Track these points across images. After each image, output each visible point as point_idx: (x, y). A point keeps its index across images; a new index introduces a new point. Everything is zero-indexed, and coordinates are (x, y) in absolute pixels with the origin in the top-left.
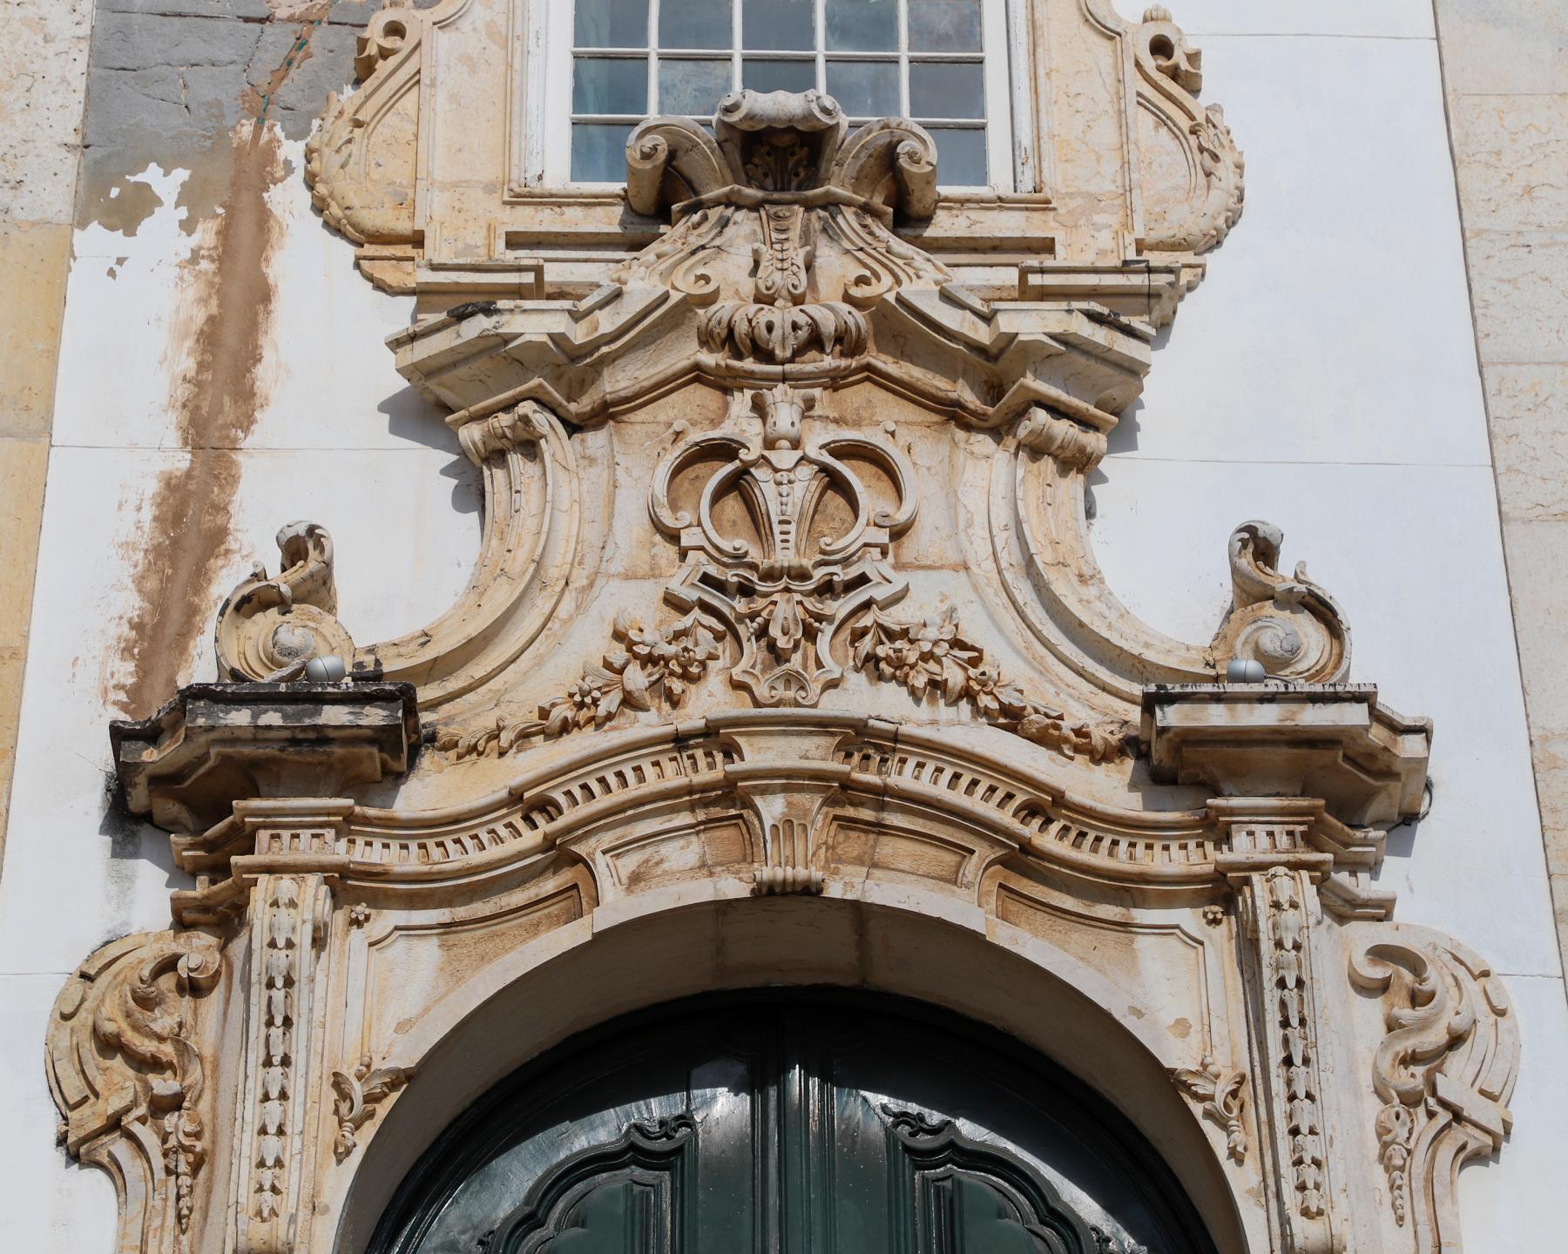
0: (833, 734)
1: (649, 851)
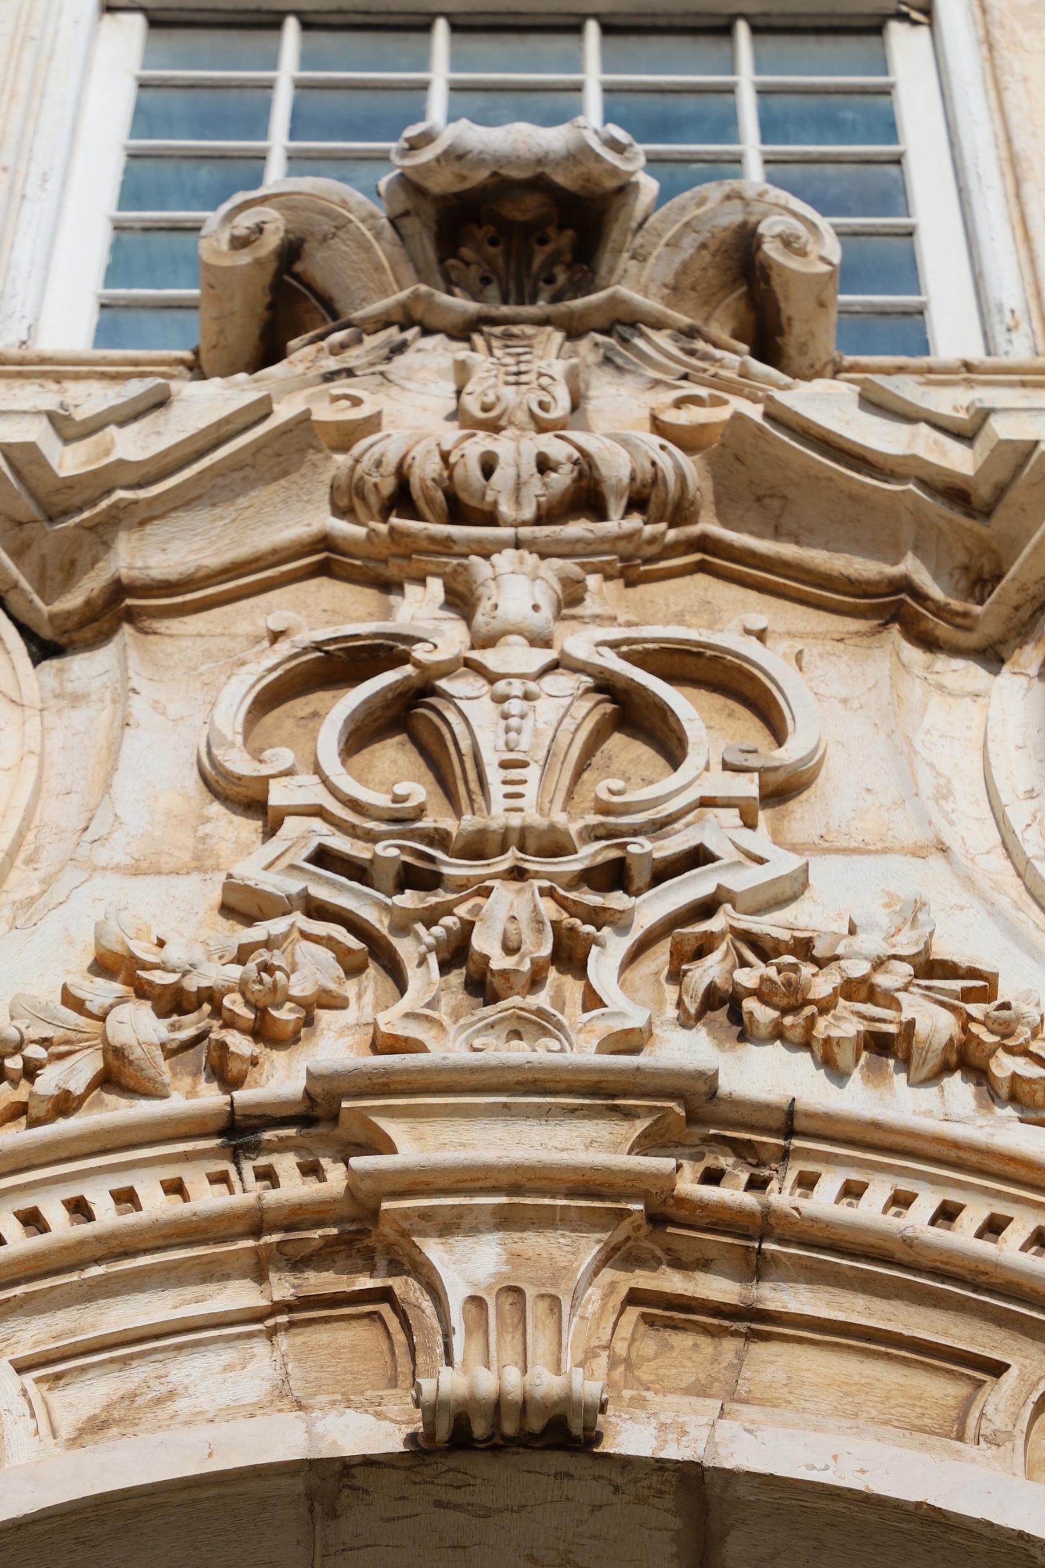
0: (628, 1114)
1: (138, 1374)
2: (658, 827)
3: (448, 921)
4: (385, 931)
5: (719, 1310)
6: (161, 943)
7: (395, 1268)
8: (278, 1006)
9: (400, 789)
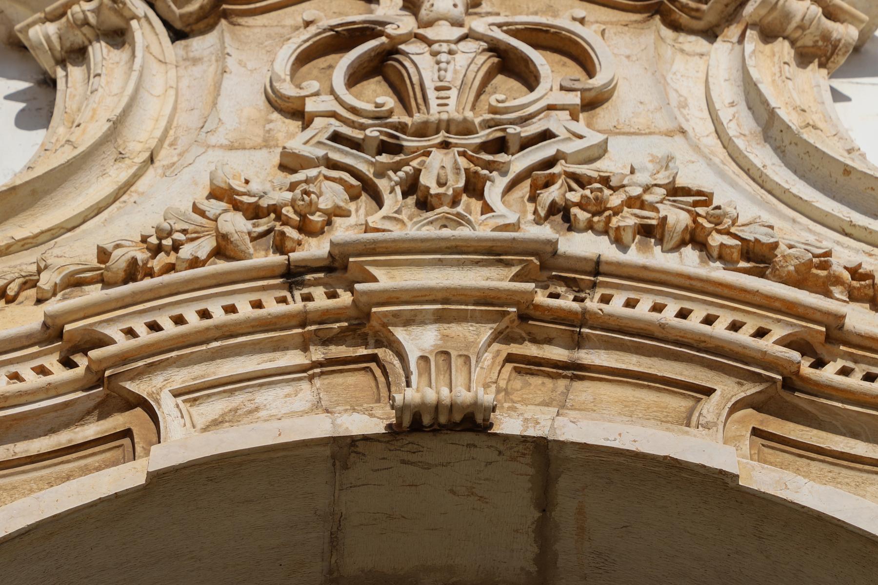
0: (508, 264)
2: (524, 121)
3: (407, 168)
4: (371, 176)
5: (556, 364)
6: (247, 182)
7: (379, 344)
8: (313, 214)
9: (380, 100)
